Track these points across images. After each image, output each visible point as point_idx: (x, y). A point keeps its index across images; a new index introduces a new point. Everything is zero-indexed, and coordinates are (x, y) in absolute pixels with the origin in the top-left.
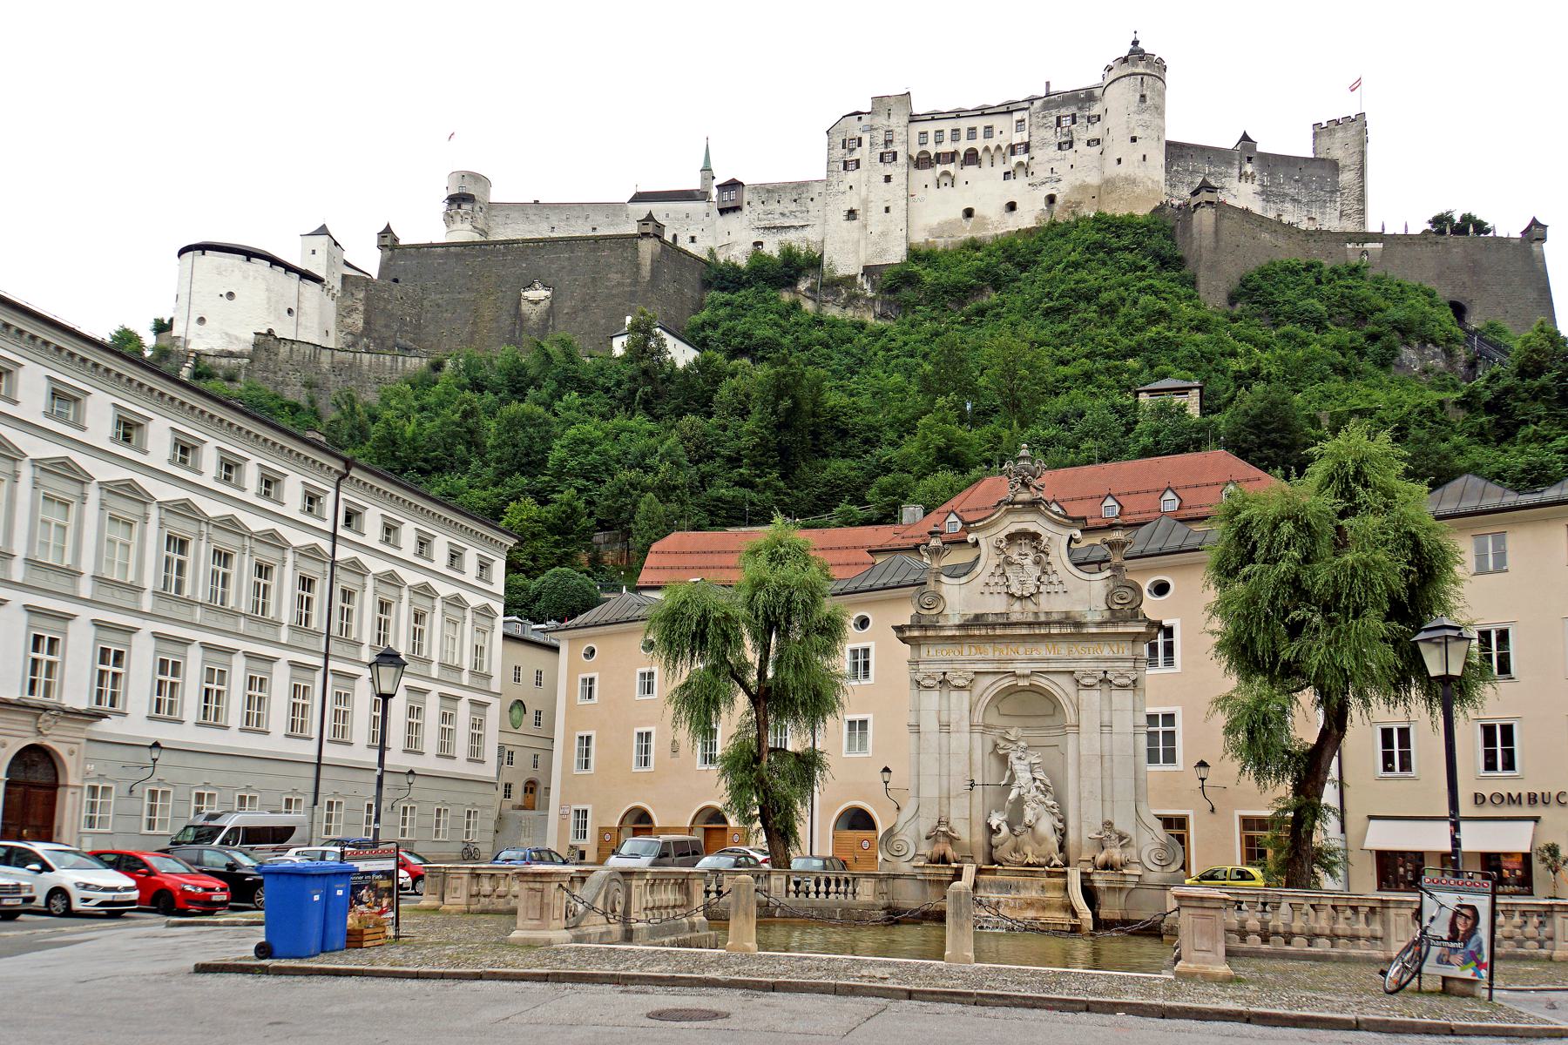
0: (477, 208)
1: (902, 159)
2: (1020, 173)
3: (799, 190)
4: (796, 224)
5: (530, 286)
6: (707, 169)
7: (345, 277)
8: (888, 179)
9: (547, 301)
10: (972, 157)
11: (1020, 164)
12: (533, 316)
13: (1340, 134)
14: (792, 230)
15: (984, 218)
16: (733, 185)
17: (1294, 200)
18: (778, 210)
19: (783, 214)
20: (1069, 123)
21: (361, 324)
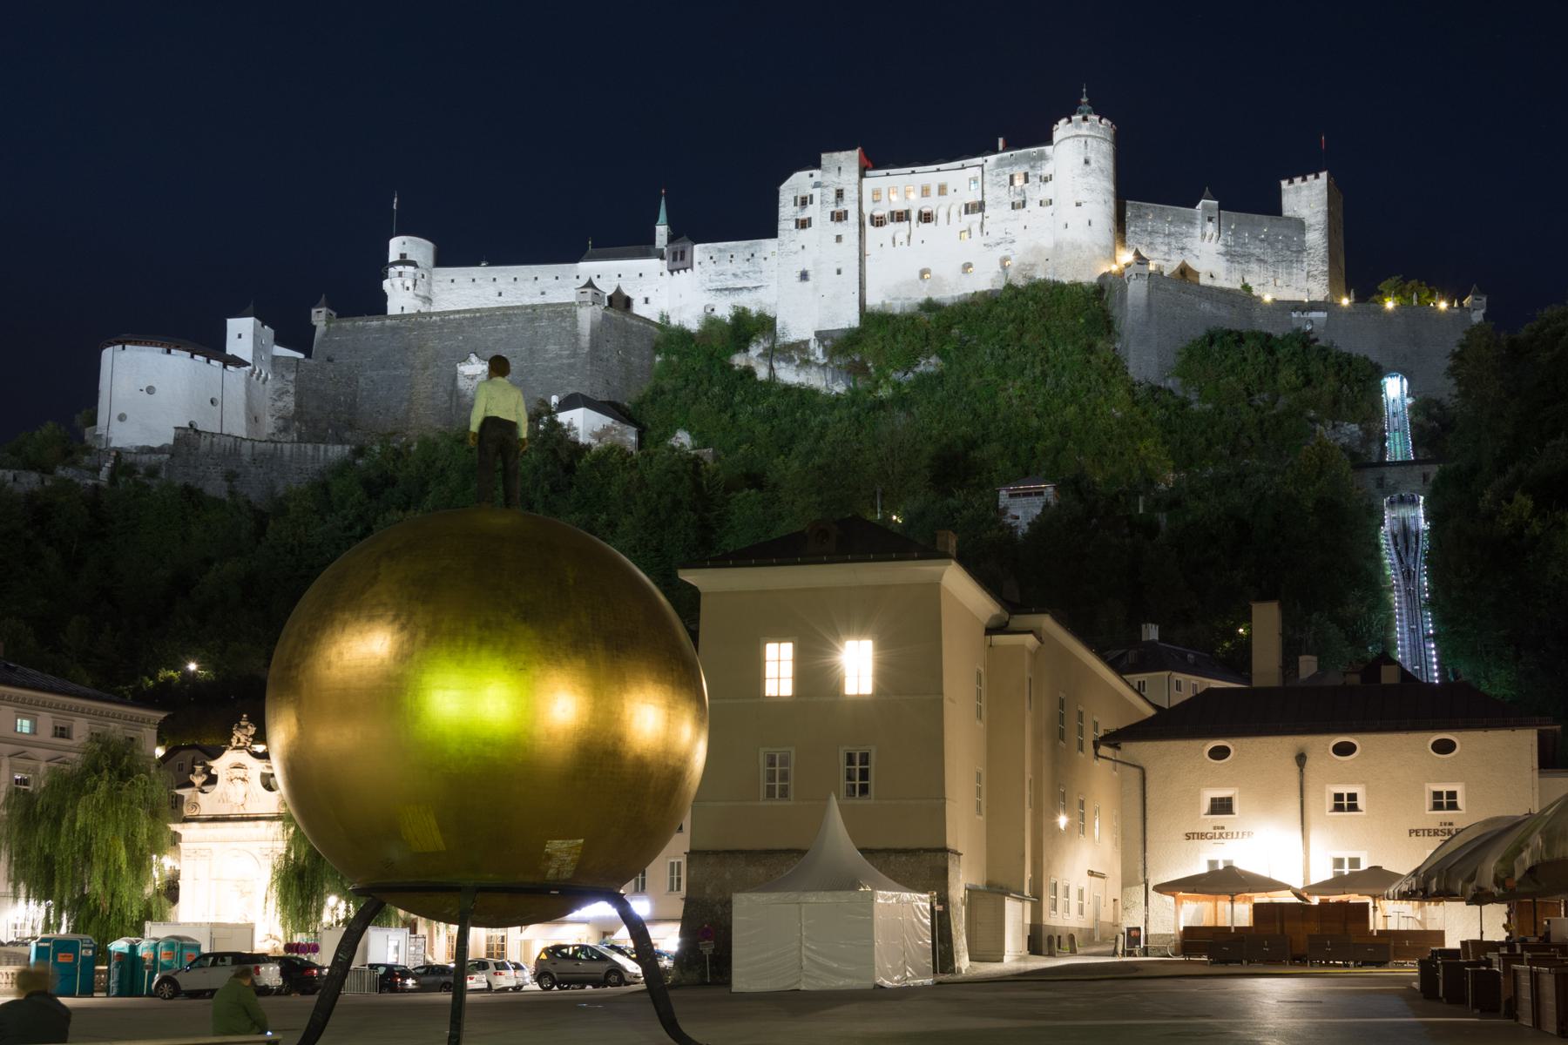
4: (749, 284)
5: (465, 359)
8: (839, 239)
10: (926, 218)
13: (1305, 193)
14: (745, 292)
17: (1260, 260)
19: (735, 275)
20: (1022, 181)
21: (292, 406)
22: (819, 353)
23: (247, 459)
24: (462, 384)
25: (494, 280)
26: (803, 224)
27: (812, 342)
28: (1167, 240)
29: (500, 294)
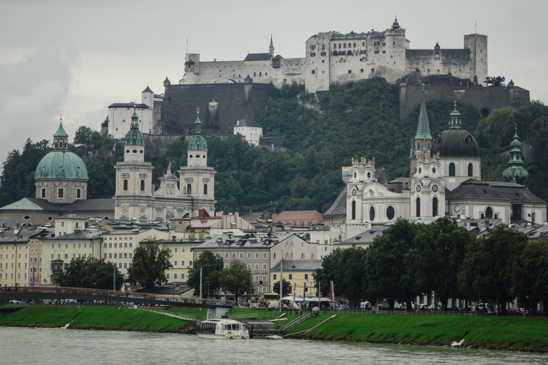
0: (195, 66)
1: (327, 54)
2: (364, 60)
3: (297, 61)
4: (297, 73)
5: (211, 101)
6: (271, 47)
7: (155, 102)
8: (323, 61)
9: (217, 106)
10: (350, 53)
11: (363, 57)
12: (212, 112)
13: (470, 40)
14: (296, 75)
15: (354, 74)
16: (278, 58)
17: (455, 64)
18: (291, 68)
19: (293, 70)
21: (160, 117)
22: (317, 98)
23: (151, 141)
24: (210, 108)
25: (219, 66)
26: (313, 55)
27: (316, 95)
28: (423, 61)
29: (220, 71)
